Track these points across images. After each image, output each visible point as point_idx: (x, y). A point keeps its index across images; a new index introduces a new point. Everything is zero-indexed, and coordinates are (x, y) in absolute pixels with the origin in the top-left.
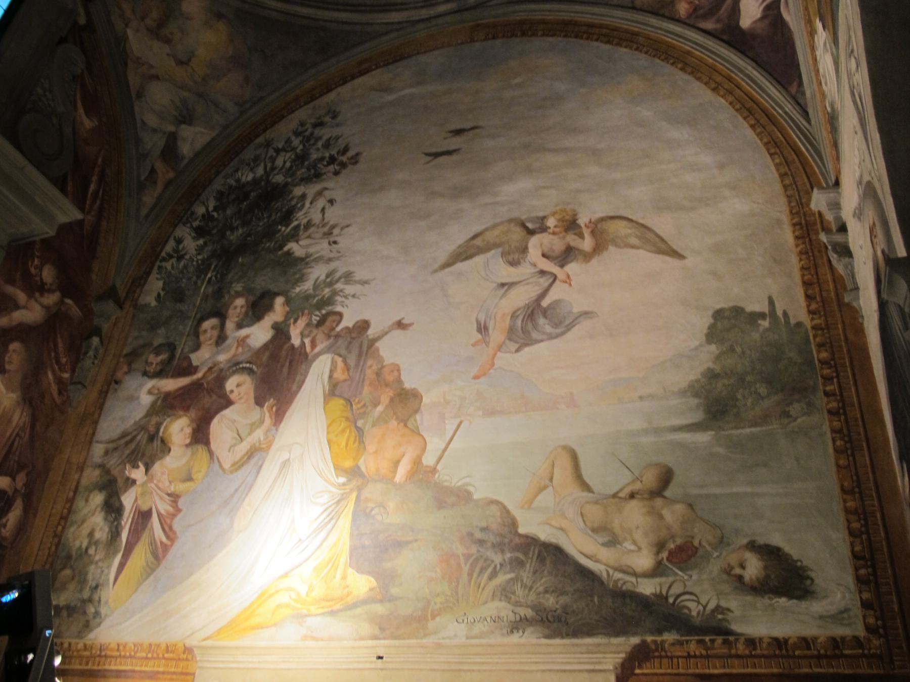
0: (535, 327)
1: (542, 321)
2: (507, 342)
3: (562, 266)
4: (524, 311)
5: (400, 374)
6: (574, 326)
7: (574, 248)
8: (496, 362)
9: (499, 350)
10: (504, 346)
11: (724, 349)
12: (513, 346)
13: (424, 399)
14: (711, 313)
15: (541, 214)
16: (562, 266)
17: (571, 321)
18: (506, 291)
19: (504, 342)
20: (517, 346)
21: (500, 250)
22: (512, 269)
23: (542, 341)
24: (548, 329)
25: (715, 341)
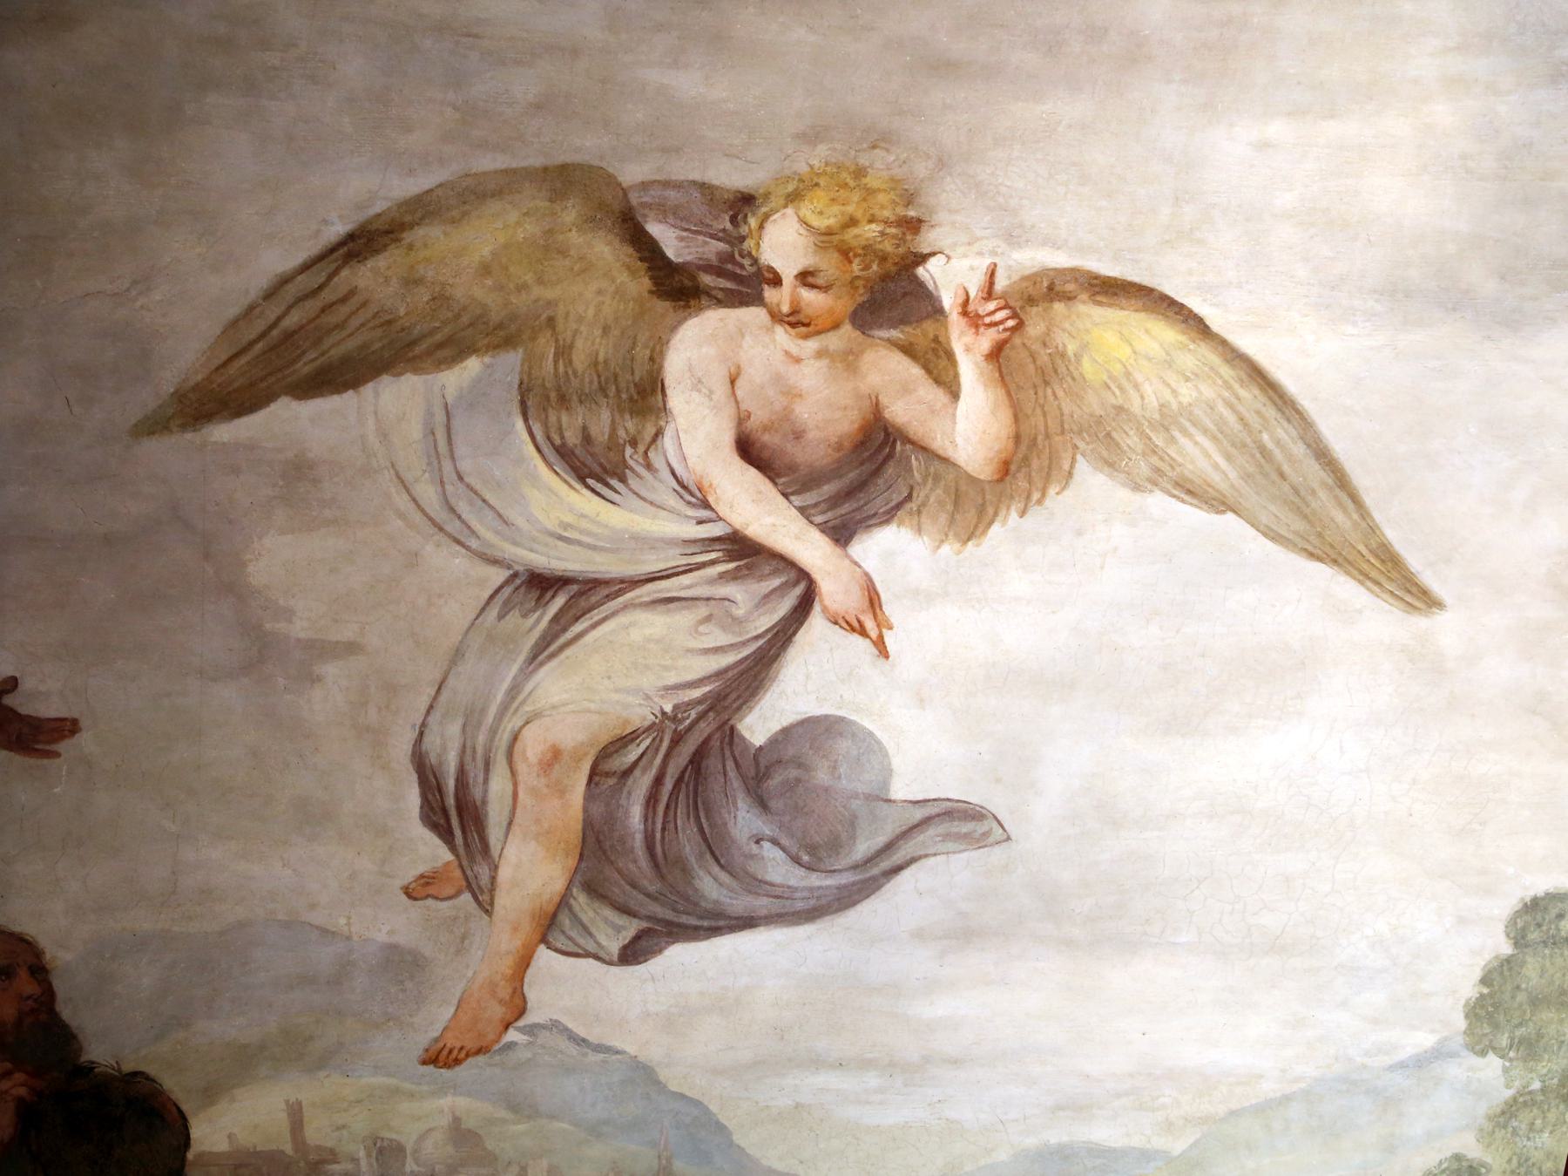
0: (715, 848)
1: (744, 821)
2: (581, 900)
3: (841, 534)
4: (653, 748)
5: (49, 994)
6: (897, 869)
7: (907, 440)
8: (532, 994)
9: (544, 940)
10: (565, 920)
11: (1536, 1085)
12: (612, 932)
13: (196, 1132)
14: (1505, 905)
15: (730, 177)
16: (841, 534)
17: (881, 840)
18: (561, 622)
19: (564, 902)
20: (632, 927)
21: (510, 363)
22: (581, 502)
23: (747, 922)
24: (776, 867)
25: (1504, 1041)
